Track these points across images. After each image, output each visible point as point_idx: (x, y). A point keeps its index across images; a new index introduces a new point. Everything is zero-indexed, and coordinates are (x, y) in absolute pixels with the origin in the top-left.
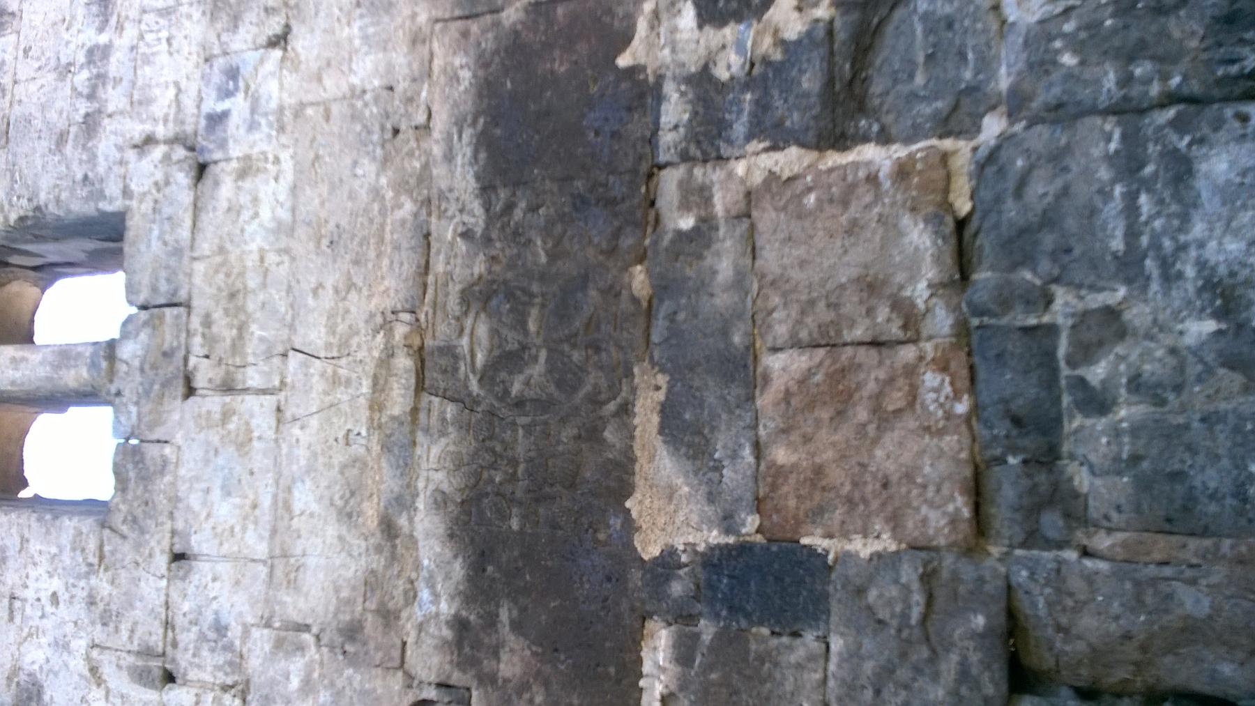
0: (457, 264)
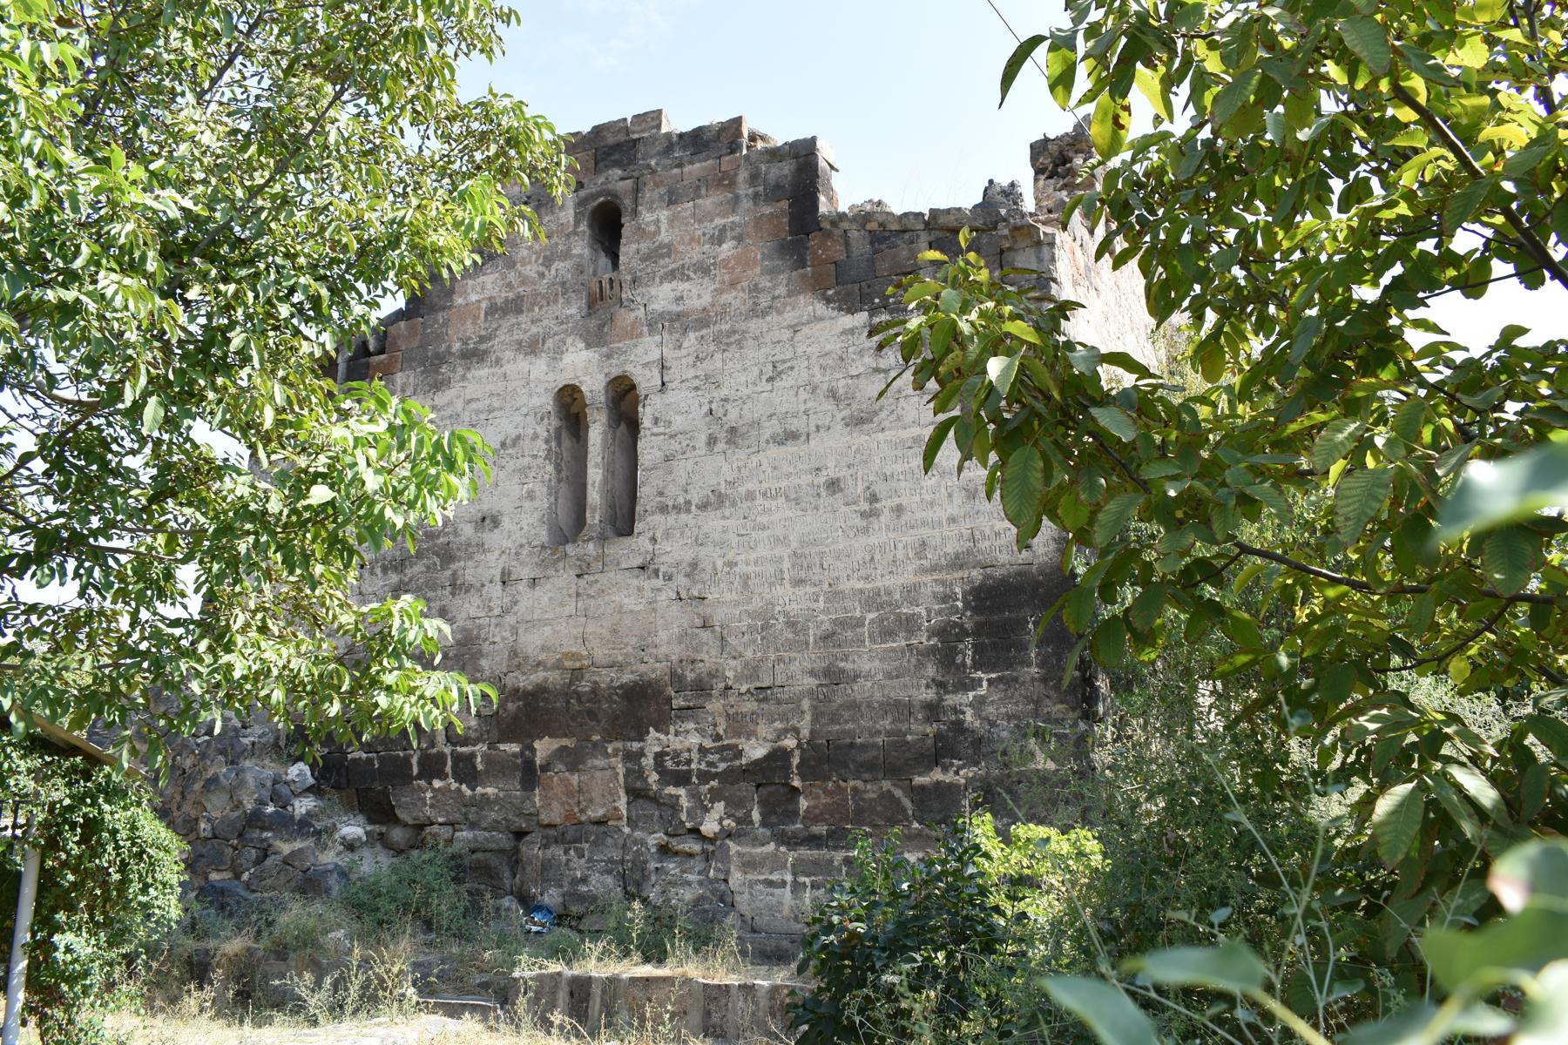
0: (606, 677)
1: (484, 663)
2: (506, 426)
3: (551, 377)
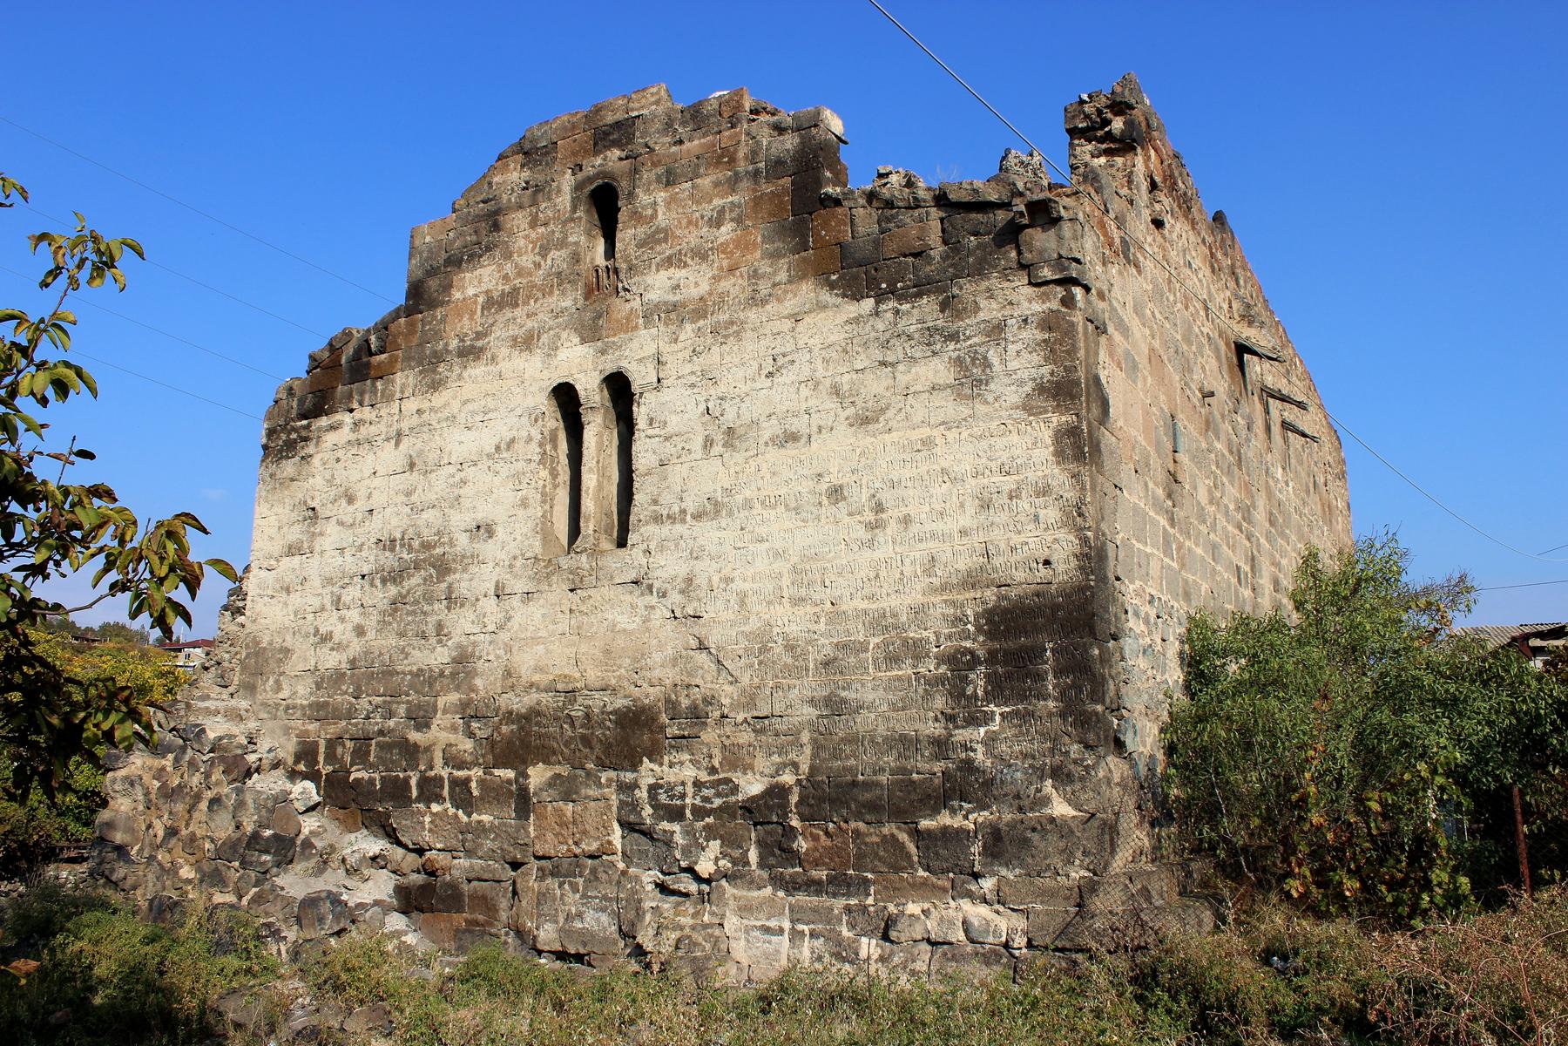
0: (597, 701)
1: (479, 682)
2: (501, 428)
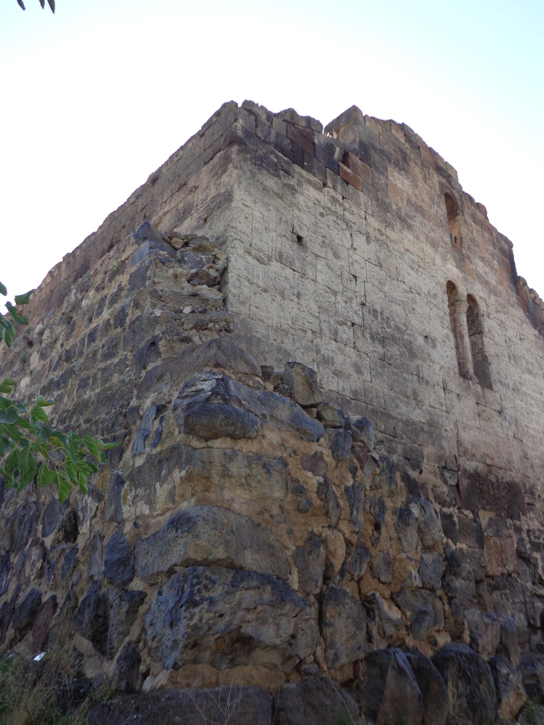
1: (444, 443)
3: (443, 269)
